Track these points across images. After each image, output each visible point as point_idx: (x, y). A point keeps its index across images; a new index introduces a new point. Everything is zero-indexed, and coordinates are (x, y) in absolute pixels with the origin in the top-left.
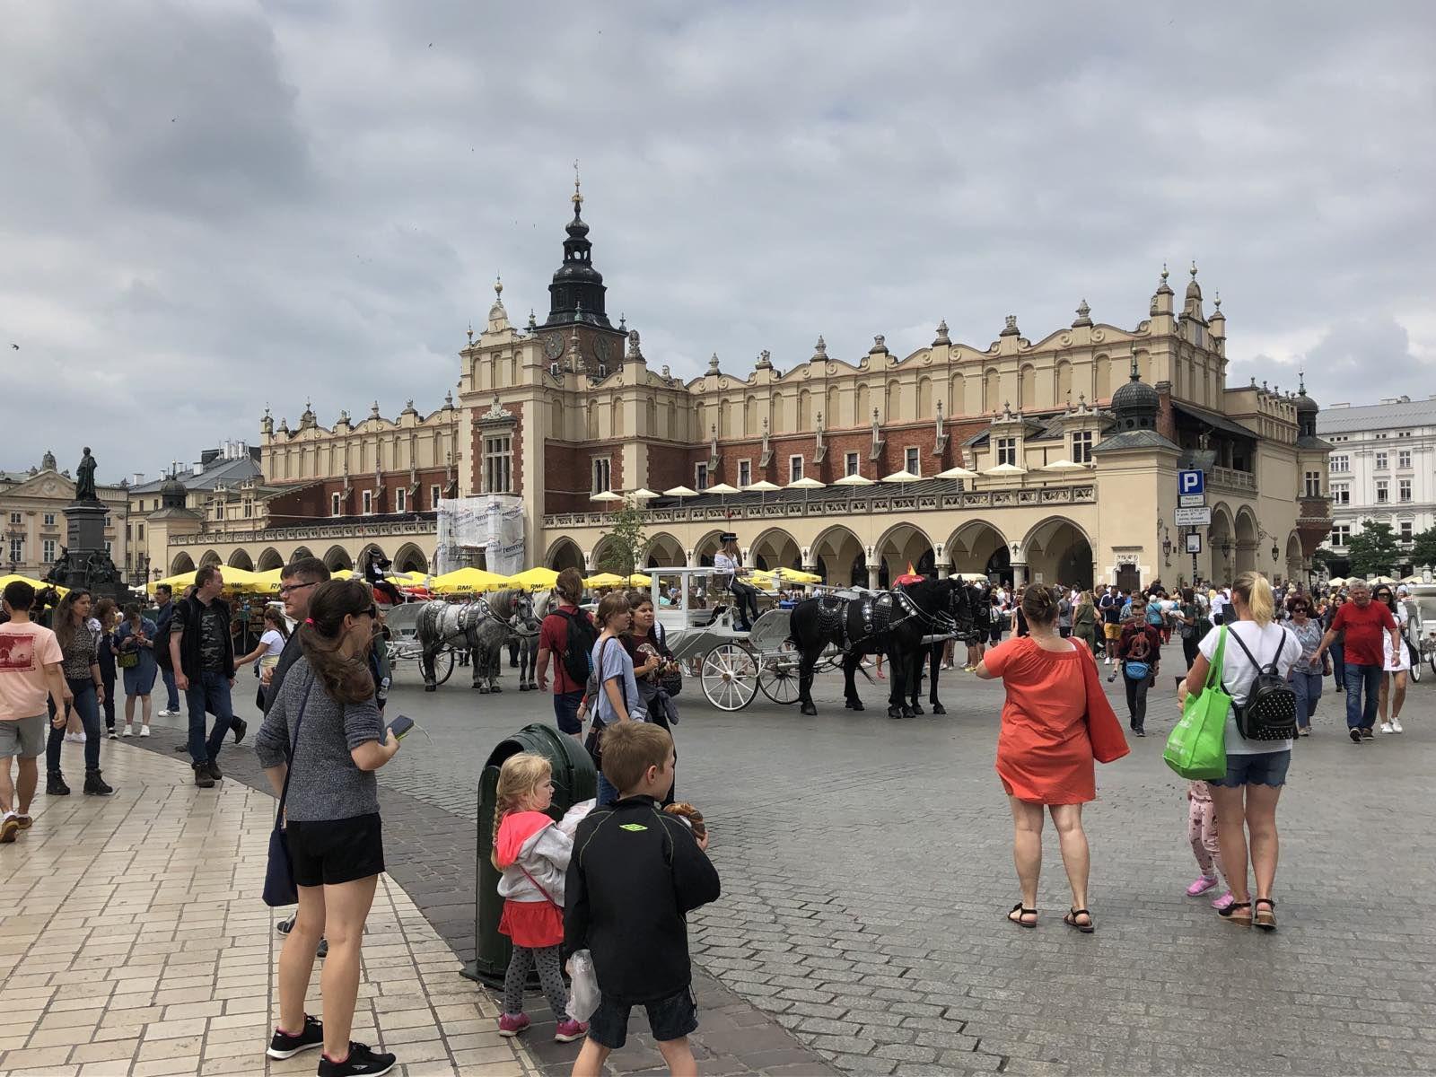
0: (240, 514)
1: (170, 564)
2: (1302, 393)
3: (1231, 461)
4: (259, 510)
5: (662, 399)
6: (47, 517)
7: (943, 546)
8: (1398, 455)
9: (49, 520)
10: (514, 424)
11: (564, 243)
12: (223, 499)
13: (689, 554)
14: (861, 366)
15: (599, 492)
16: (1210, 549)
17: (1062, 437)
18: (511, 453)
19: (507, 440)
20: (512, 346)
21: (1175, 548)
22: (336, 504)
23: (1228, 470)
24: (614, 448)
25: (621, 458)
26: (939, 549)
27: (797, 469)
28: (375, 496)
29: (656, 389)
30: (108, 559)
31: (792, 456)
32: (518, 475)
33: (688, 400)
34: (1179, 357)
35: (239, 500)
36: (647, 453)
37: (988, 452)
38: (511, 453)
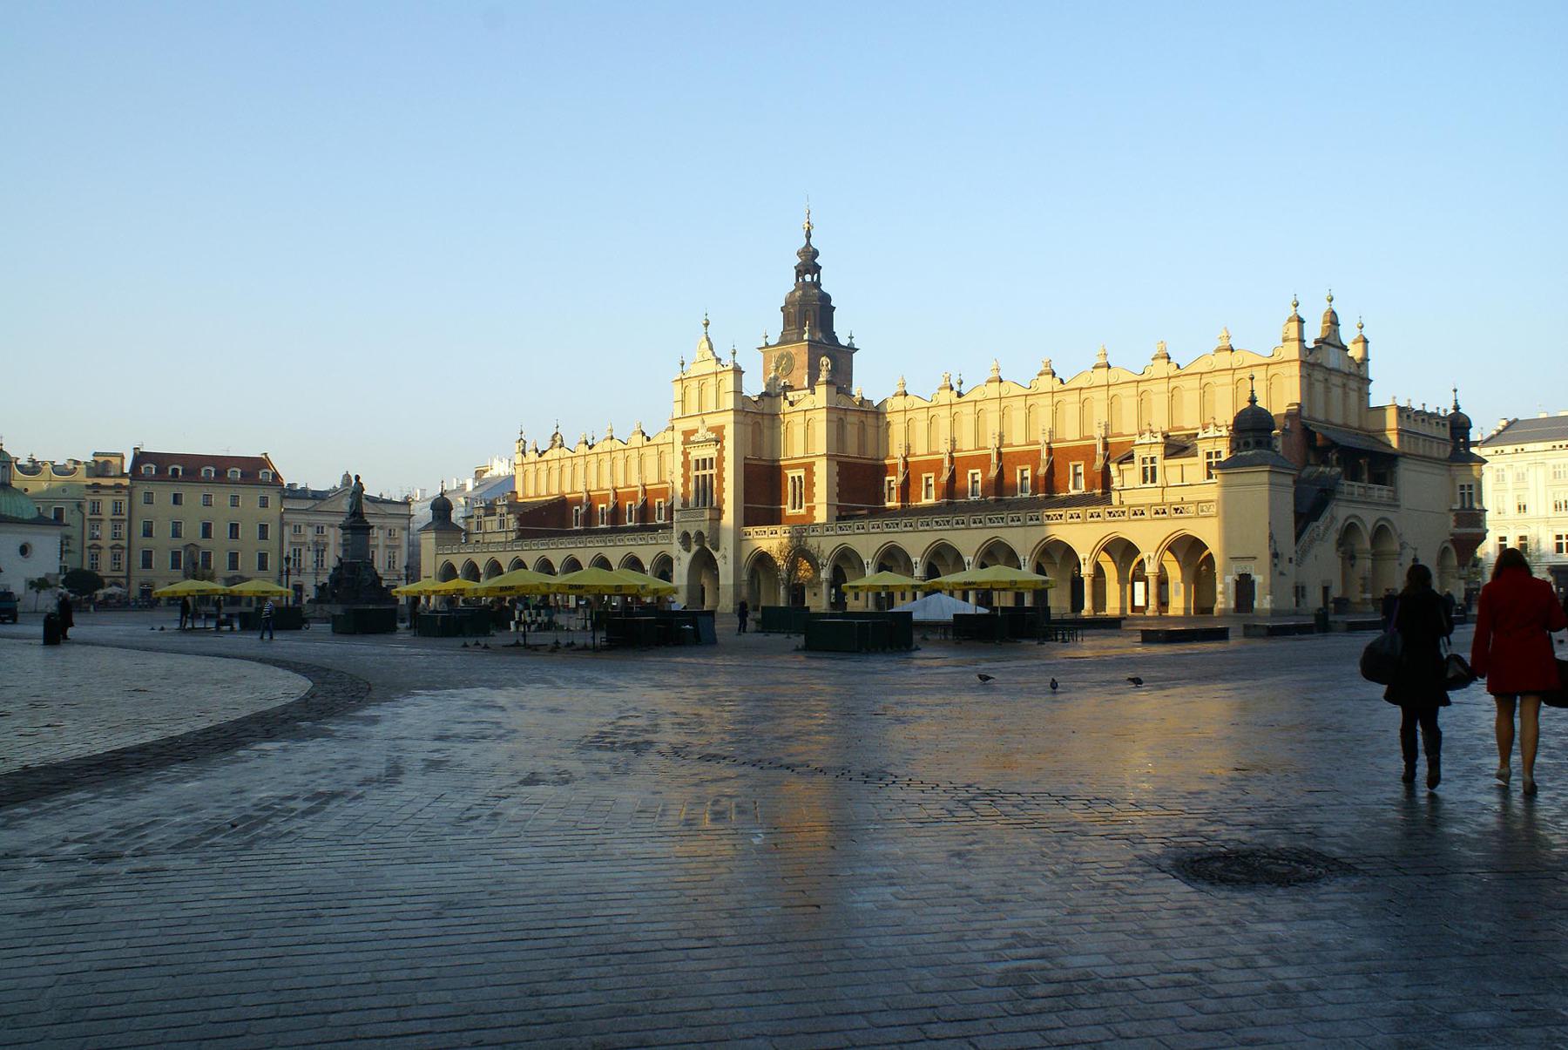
0: (495, 526)
2: (1457, 408)
3: (1365, 477)
4: (511, 525)
5: (852, 419)
7: (1087, 556)
8: (1494, 471)
12: (482, 512)
13: (868, 564)
15: (794, 508)
16: (1340, 560)
17: (1195, 455)
18: (714, 471)
19: (711, 459)
21: (1290, 560)
22: (577, 517)
23: (1360, 484)
24: (809, 468)
25: (814, 474)
26: (1084, 560)
28: (609, 509)
30: (373, 567)
31: (971, 471)
32: (721, 490)
33: (878, 419)
35: (494, 514)
38: (714, 471)
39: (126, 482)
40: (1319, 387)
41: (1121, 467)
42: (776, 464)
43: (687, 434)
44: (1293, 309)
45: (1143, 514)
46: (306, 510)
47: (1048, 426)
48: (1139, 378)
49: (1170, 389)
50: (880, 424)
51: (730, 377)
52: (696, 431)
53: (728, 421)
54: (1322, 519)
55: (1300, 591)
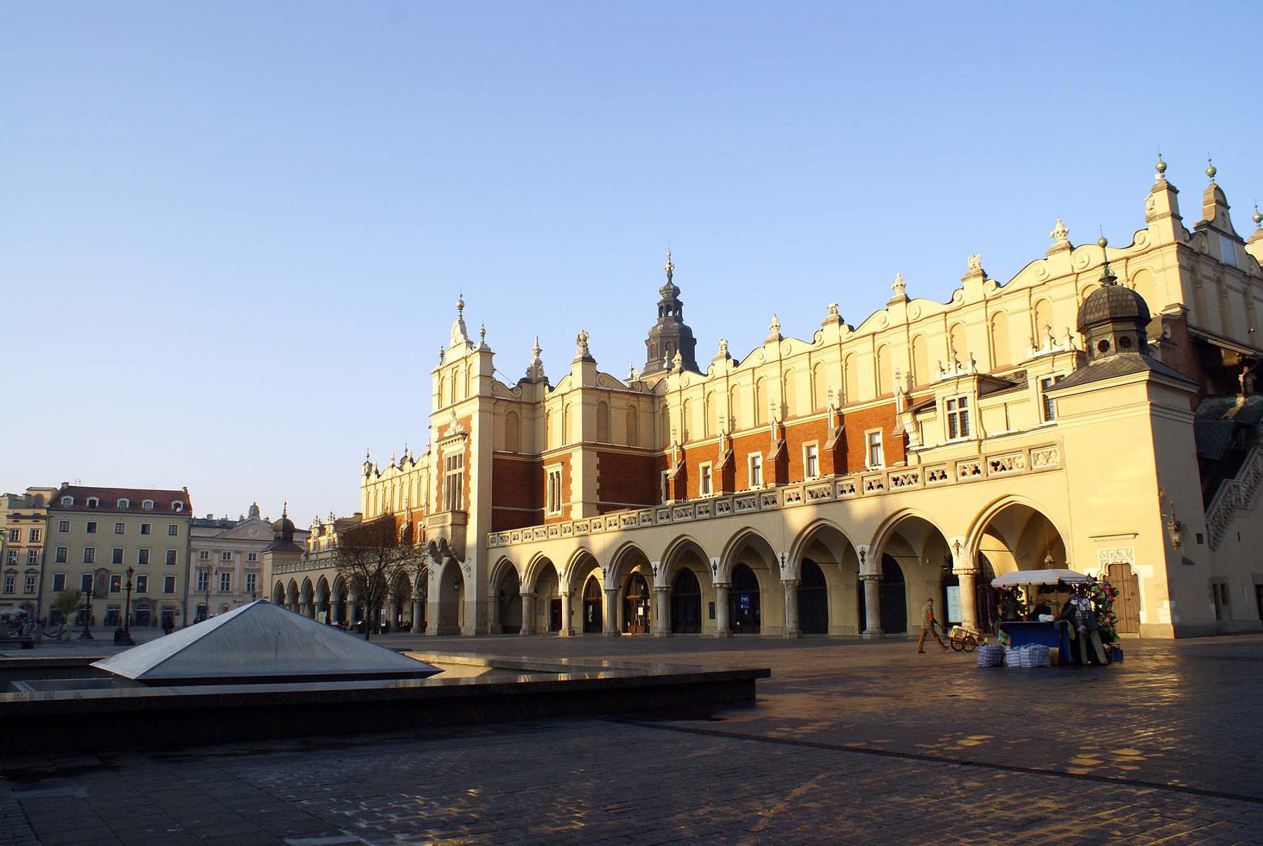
1: (273, 590)
5: (618, 402)
6: (250, 555)
7: (867, 548)
9: (252, 557)
10: (464, 439)
11: (658, 304)
14: (815, 342)
15: (553, 510)
18: (462, 470)
20: (466, 358)
21: (1199, 537)
24: (565, 461)
26: (863, 554)
27: (755, 468)
29: (609, 391)
32: (468, 490)
33: (653, 403)
34: (1199, 277)
36: (597, 461)
37: (935, 418)
39: (44, 512)
40: (1210, 288)
41: (919, 417)
42: (538, 460)
43: (442, 429)
44: (1158, 176)
45: (944, 476)
46: (212, 537)
47: (836, 388)
48: (946, 308)
49: (990, 317)
50: (657, 408)
51: (476, 360)
52: (447, 426)
53: (473, 408)
54: (1241, 476)
55: (1220, 592)
